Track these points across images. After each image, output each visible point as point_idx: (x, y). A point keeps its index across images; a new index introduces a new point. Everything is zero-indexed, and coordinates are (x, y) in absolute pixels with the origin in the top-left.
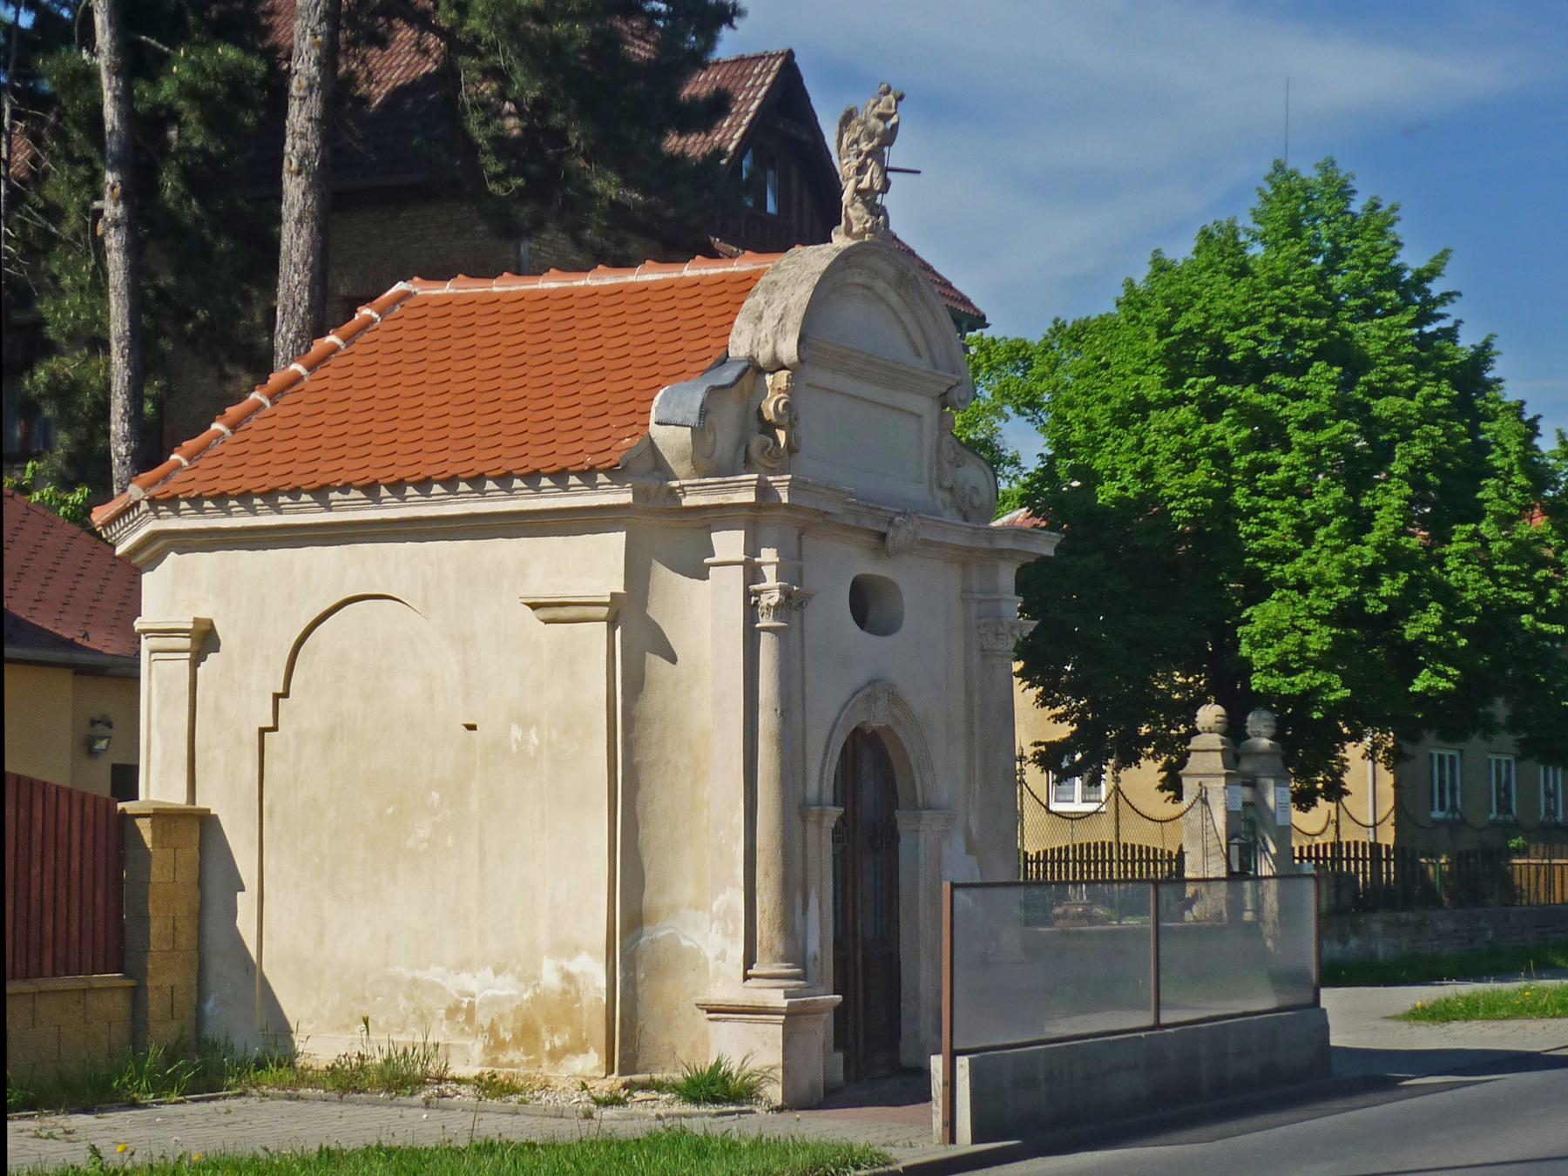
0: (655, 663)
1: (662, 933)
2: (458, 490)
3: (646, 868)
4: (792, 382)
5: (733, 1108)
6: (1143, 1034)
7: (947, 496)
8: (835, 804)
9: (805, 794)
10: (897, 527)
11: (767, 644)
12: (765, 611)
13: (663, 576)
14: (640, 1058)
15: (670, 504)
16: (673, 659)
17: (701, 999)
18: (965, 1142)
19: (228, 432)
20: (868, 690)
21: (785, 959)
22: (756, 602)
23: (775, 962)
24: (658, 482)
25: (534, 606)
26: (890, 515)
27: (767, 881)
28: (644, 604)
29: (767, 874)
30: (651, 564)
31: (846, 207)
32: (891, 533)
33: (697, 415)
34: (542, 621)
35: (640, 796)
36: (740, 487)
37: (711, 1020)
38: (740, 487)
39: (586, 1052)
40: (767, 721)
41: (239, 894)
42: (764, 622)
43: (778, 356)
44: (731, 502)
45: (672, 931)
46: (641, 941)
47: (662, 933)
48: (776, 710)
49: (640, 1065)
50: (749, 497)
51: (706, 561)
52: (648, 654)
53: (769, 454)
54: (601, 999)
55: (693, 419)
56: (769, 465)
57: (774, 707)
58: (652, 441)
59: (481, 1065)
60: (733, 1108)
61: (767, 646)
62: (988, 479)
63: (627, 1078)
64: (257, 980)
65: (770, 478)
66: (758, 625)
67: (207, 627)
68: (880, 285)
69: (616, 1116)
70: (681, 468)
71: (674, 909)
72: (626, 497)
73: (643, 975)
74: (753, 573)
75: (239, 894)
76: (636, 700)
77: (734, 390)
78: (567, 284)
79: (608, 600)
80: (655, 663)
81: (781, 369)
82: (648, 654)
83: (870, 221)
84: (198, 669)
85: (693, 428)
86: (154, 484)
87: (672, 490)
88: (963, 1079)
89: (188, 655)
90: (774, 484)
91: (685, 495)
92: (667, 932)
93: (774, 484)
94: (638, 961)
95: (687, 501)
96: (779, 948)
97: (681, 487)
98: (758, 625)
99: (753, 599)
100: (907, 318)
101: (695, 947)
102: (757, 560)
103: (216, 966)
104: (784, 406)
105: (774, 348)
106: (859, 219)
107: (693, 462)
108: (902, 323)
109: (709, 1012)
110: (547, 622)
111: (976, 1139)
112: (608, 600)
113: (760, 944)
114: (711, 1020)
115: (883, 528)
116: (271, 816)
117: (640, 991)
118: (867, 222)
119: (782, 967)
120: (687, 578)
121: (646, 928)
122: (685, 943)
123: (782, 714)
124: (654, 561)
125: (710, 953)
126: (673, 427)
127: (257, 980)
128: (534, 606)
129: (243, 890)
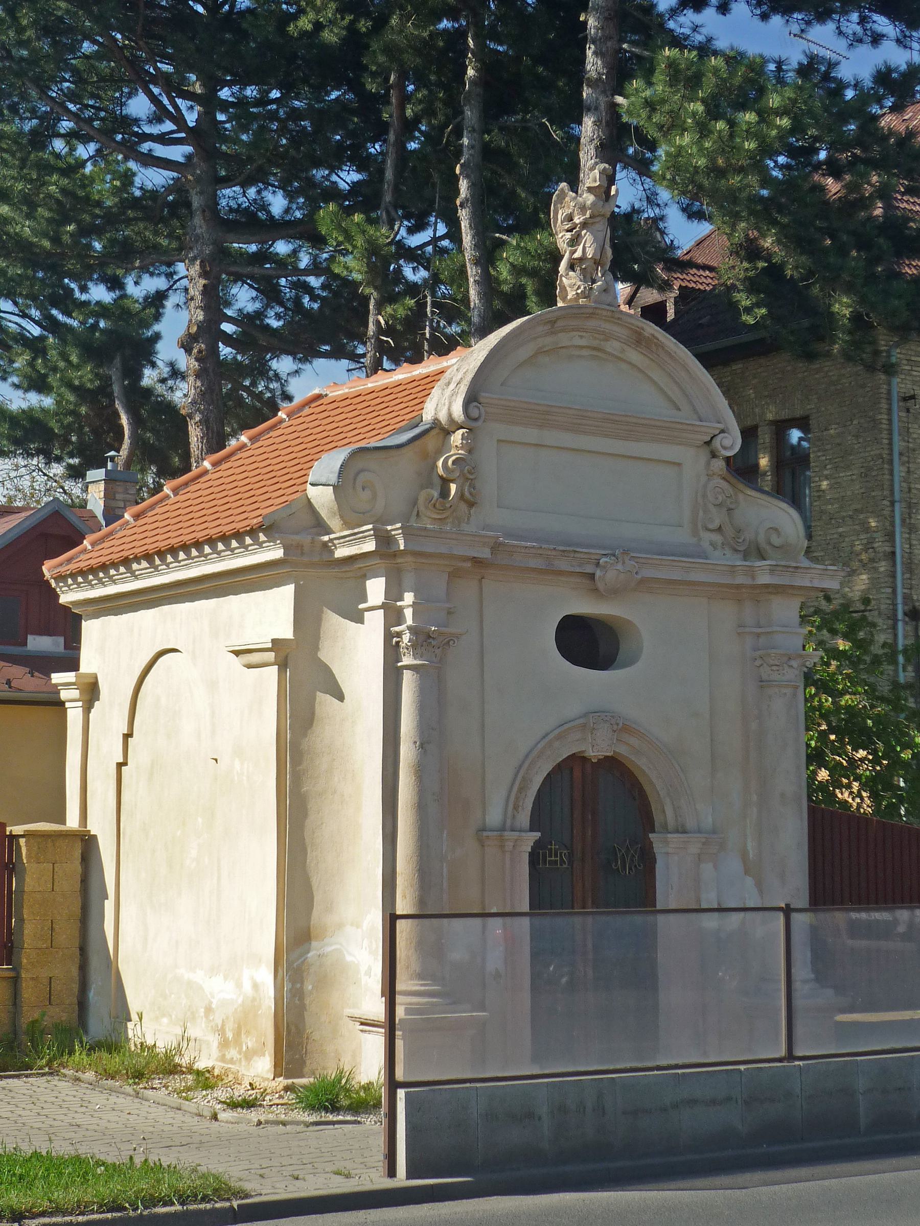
0: (325, 701)
1: (329, 949)
2: (180, 559)
3: (315, 888)
4: (467, 439)
5: (349, 1118)
6: (742, 1067)
7: (717, 538)
8: (532, 830)
9: (484, 820)
10: (604, 568)
11: (409, 681)
12: (406, 650)
13: (333, 621)
14: (308, 1062)
15: (326, 557)
16: (341, 697)
17: (357, 1013)
18: (402, 1179)
19: (132, 520)
20: (582, 721)
21: (420, 976)
22: (398, 643)
23: (411, 979)
24: (309, 537)
25: (237, 653)
26: (596, 557)
27: (404, 902)
28: (315, 645)
29: (404, 897)
30: (322, 612)
31: (562, 276)
32: (598, 573)
33: (337, 475)
34: (245, 666)
35: (309, 823)
36: (365, 537)
37: (362, 1031)
38: (365, 537)
39: (264, 1055)
40: (407, 752)
41: (106, 901)
42: (407, 660)
43: (453, 416)
44: (362, 552)
45: (337, 946)
46: (309, 955)
47: (329, 949)
48: (415, 742)
49: (306, 1070)
50: (370, 546)
51: (361, 606)
52: (318, 693)
53: (434, 506)
54: (271, 1007)
55: (333, 479)
56: (439, 517)
57: (413, 740)
58: (309, 500)
59: (217, 1060)
60: (349, 1118)
61: (409, 684)
62: (793, 520)
63: (290, 1081)
64: (113, 977)
65: (389, 528)
66: (399, 664)
67: (92, 680)
68: (613, 346)
69: (230, 1119)
70: (334, 523)
71: (340, 926)
72: (277, 553)
73: (310, 987)
74: (393, 615)
75: (106, 901)
76: (305, 735)
77: (408, 452)
78: (409, 375)
79: (270, 645)
80: (325, 701)
81: (458, 429)
82: (318, 693)
83: (582, 287)
84: (90, 715)
85: (334, 486)
86: (56, 567)
87: (325, 544)
88: (401, 1113)
89: (80, 704)
90: (393, 533)
91: (336, 548)
92: (333, 947)
93: (393, 533)
94: (305, 974)
95: (341, 552)
96: (416, 966)
97: (331, 540)
98: (399, 664)
99: (395, 640)
100: (656, 375)
101: (356, 962)
102: (399, 604)
103: (95, 962)
104: (454, 462)
105: (449, 409)
106: (572, 286)
107: (342, 517)
108: (654, 383)
109: (362, 1024)
110: (249, 666)
111: (410, 1176)
112: (270, 645)
113: (400, 962)
114: (362, 1031)
115: (589, 569)
116: (124, 839)
117: (307, 1002)
118: (579, 288)
119: (417, 985)
120: (353, 623)
121: (314, 944)
122: (349, 958)
123: (422, 746)
124: (325, 609)
125: (363, 969)
126: (321, 486)
127: (113, 977)
128: (237, 653)
129: (107, 899)
